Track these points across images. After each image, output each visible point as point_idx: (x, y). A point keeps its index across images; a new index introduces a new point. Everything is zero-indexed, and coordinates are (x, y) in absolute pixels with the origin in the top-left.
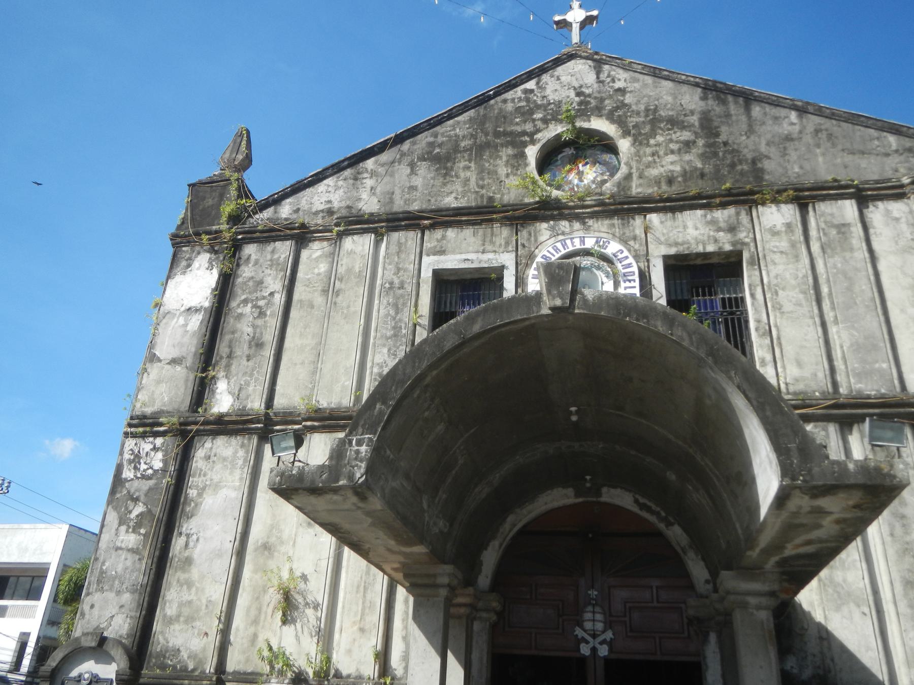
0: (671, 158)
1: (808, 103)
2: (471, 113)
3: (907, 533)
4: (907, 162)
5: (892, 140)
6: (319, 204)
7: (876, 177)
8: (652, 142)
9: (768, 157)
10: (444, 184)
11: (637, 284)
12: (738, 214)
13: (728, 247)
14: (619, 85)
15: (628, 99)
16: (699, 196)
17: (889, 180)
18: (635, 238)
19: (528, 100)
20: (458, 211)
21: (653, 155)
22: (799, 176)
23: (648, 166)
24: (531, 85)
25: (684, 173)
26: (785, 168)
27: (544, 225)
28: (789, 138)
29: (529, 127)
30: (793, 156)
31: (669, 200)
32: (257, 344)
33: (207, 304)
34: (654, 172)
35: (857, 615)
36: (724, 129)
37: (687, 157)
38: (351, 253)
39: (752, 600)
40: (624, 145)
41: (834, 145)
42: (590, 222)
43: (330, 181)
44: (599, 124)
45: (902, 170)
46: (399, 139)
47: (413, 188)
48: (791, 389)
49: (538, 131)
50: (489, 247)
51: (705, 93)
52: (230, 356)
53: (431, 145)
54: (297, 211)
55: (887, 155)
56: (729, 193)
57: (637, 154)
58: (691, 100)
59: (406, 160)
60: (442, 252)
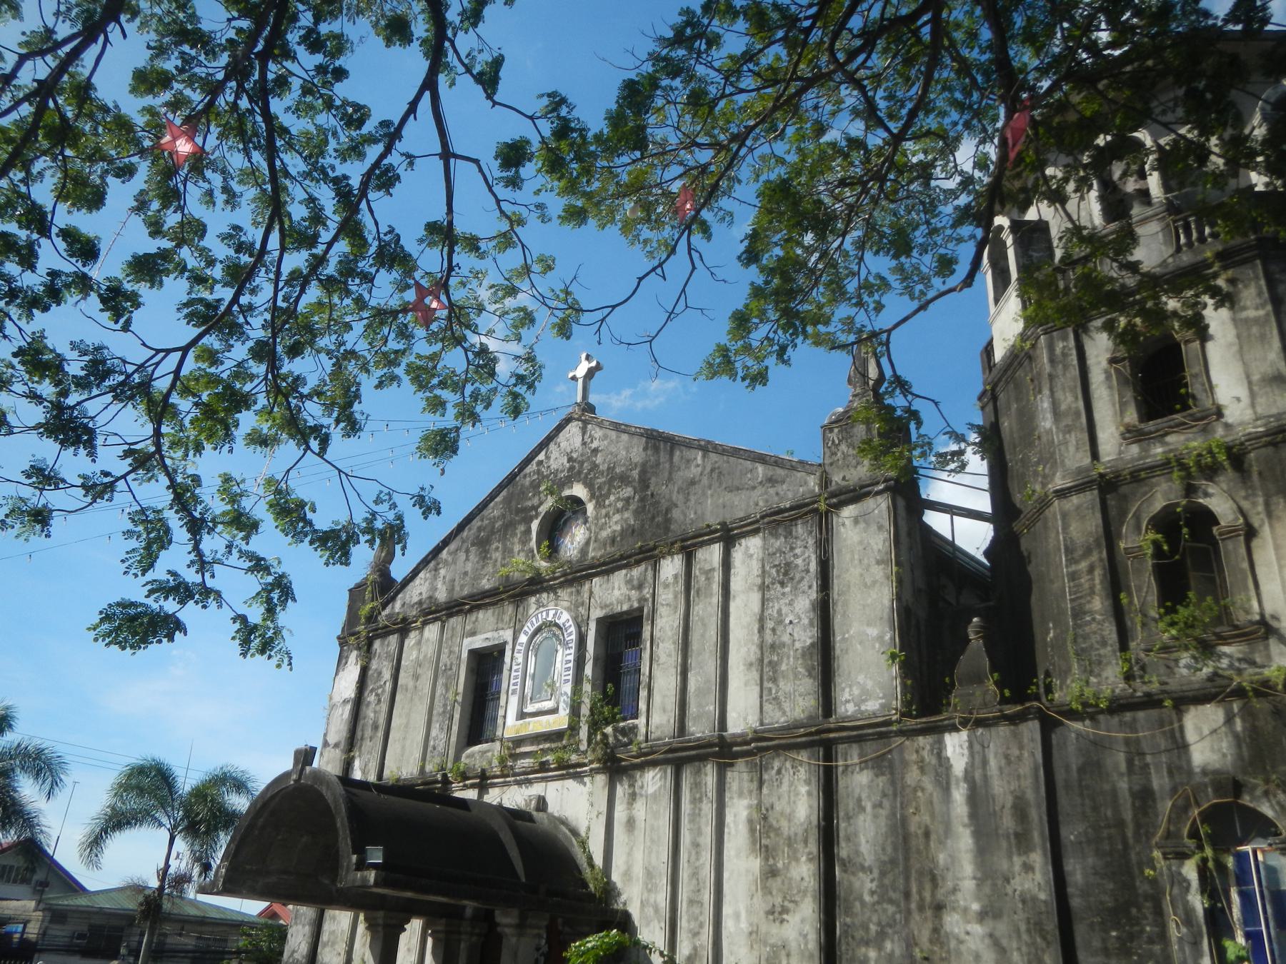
0: (617, 517)
1: (709, 442)
2: (504, 493)
3: (698, 859)
4: (766, 493)
5: (760, 469)
6: (416, 599)
7: (741, 514)
8: (607, 502)
9: (676, 506)
10: (483, 567)
11: (572, 651)
12: (646, 570)
13: (636, 605)
14: (594, 445)
15: (599, 459)
16: (622, 557)
17: (748, 517)
18: (583, 604)
19: (538, 472)
20: (485, 594)
21: (607, 515)
22: (693, 522)
23: (601, 529)
24: (541, 457)
25: (623, 533)
26: (685, 515)
27: (533, 599)
28: (693, 483)
29: (535, 501)
30: (693, 498)
31: (604, 564)
32: (375, 727)
33: (353, 696)
34: (604, 534)
35: (657, 928)
36: (653, 480)
37: (626, 515)
38: (428, 640)
39: (507, 930)
40: (590, 507)
41: (721, 484)
42: (560, 592)
43: (422, 575)
44: (579, 491)
45: (761, 503)
46: (461, 527)
47: (466, 573)
48: (653, 736)
49: (541, 503)
50: (500, 625)
51: (647, 443)
52: (362, 739)
53: (480, 529)
54: (403, 605)
55: (754, 488)
56: (641, 550)
57: (597, 518)
58: (636, 452)
59: (465, 546)
60: (473, 633)
